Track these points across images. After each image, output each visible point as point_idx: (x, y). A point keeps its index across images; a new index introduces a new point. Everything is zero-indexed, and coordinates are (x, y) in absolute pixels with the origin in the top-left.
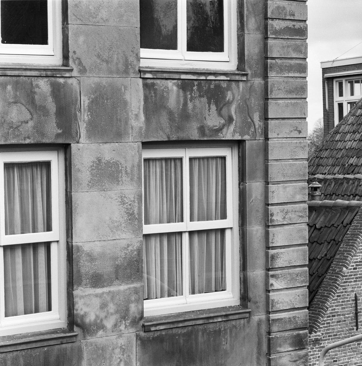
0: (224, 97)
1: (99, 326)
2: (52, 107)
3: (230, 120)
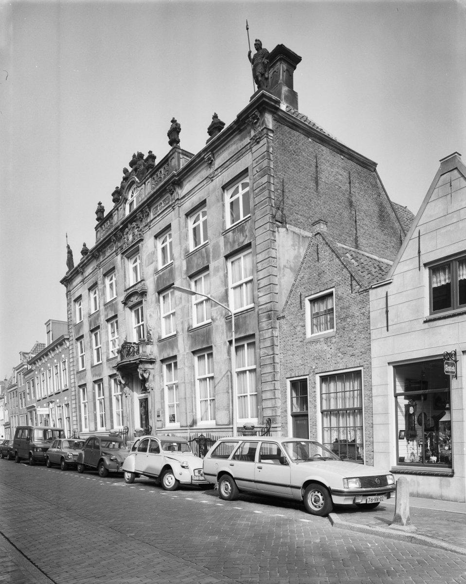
0: (244, 228)
1: (217, 319)
2: (205, 255)
3: (246, 236)
